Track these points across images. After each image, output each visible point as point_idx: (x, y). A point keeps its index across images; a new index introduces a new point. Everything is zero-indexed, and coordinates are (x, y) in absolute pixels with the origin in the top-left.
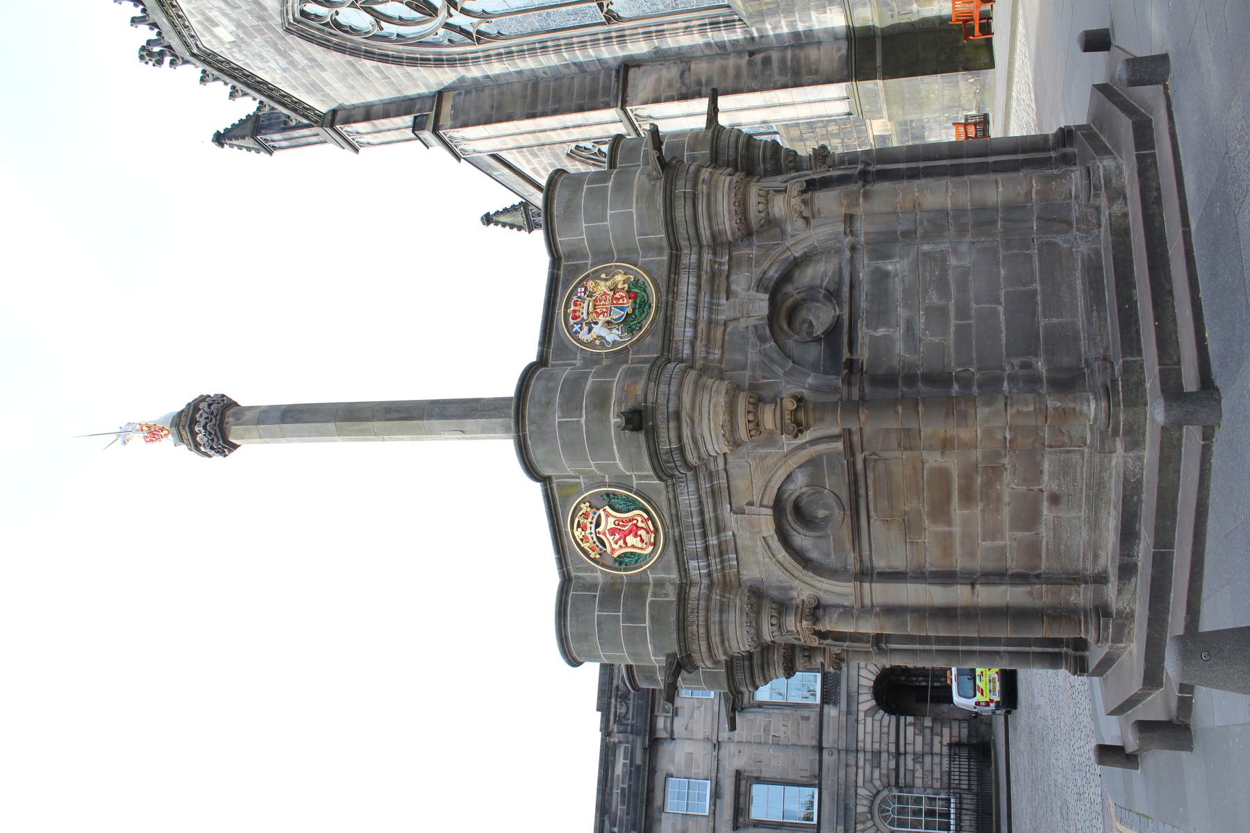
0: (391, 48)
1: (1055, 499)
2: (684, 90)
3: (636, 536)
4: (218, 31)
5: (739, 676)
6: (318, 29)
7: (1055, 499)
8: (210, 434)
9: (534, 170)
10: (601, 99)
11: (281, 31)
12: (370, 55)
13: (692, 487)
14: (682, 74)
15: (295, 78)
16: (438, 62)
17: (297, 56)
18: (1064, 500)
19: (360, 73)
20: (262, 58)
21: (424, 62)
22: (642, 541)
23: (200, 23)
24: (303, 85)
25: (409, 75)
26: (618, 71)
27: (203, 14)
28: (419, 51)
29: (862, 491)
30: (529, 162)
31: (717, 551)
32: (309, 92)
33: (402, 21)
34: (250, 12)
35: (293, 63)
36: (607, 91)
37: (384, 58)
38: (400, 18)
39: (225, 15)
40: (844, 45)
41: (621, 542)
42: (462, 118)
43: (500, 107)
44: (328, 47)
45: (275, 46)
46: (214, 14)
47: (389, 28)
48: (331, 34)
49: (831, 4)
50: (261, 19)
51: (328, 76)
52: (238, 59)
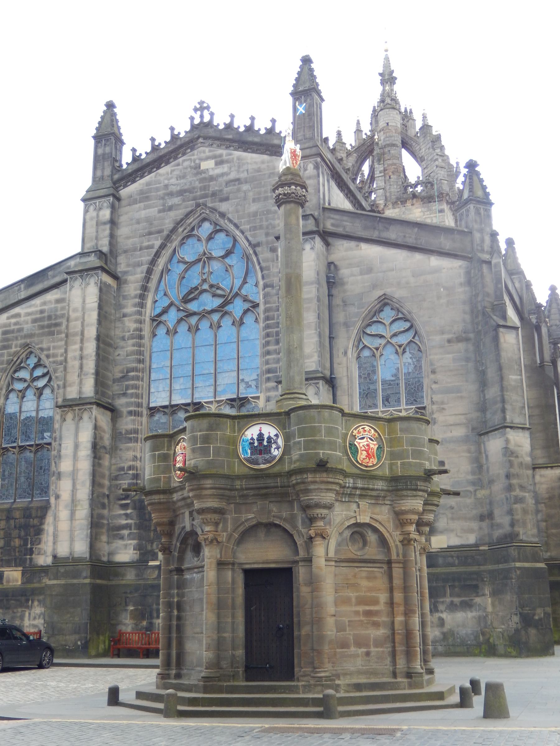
0: (161, 262)
1: (368, 654)
2: (98, 447)
3: (366, 456)
5: (223, 481)
6: (191, 223)
7: (368, 654)
8: (300, 196)
9: (18, 315)
11: (201, 201)
12: (163, 246)
13: (385, 488)
14: (105, 448)
15: (157, 189)
16: (145, 288)
17: (176, 200)
18: (367, 658)
19: (150, 233)
21: (147, 279)
23: (221, 156)
24: (150, 191)
25: (139, 264)
26: (110, 404)
27: (227, 162)
28: (155, 277)
29: (369, 565)
30: (28, 314)
31: (353, 493)
32: (141, 192)
34: (221, 191)
35: (171, 194)
37: (157, 255)
38: (184, 277)
39: (222, 175)
40: (105, 559)
41: (363, 448)
42: (104, 289)
43: (106, 317)
44: (178, 224)
45: (190, 191)
46: (225, 168)
48: (185, 229)
49: (140, 554)
50: (214, 194)
51: (153, 212)
52: (184, 162)
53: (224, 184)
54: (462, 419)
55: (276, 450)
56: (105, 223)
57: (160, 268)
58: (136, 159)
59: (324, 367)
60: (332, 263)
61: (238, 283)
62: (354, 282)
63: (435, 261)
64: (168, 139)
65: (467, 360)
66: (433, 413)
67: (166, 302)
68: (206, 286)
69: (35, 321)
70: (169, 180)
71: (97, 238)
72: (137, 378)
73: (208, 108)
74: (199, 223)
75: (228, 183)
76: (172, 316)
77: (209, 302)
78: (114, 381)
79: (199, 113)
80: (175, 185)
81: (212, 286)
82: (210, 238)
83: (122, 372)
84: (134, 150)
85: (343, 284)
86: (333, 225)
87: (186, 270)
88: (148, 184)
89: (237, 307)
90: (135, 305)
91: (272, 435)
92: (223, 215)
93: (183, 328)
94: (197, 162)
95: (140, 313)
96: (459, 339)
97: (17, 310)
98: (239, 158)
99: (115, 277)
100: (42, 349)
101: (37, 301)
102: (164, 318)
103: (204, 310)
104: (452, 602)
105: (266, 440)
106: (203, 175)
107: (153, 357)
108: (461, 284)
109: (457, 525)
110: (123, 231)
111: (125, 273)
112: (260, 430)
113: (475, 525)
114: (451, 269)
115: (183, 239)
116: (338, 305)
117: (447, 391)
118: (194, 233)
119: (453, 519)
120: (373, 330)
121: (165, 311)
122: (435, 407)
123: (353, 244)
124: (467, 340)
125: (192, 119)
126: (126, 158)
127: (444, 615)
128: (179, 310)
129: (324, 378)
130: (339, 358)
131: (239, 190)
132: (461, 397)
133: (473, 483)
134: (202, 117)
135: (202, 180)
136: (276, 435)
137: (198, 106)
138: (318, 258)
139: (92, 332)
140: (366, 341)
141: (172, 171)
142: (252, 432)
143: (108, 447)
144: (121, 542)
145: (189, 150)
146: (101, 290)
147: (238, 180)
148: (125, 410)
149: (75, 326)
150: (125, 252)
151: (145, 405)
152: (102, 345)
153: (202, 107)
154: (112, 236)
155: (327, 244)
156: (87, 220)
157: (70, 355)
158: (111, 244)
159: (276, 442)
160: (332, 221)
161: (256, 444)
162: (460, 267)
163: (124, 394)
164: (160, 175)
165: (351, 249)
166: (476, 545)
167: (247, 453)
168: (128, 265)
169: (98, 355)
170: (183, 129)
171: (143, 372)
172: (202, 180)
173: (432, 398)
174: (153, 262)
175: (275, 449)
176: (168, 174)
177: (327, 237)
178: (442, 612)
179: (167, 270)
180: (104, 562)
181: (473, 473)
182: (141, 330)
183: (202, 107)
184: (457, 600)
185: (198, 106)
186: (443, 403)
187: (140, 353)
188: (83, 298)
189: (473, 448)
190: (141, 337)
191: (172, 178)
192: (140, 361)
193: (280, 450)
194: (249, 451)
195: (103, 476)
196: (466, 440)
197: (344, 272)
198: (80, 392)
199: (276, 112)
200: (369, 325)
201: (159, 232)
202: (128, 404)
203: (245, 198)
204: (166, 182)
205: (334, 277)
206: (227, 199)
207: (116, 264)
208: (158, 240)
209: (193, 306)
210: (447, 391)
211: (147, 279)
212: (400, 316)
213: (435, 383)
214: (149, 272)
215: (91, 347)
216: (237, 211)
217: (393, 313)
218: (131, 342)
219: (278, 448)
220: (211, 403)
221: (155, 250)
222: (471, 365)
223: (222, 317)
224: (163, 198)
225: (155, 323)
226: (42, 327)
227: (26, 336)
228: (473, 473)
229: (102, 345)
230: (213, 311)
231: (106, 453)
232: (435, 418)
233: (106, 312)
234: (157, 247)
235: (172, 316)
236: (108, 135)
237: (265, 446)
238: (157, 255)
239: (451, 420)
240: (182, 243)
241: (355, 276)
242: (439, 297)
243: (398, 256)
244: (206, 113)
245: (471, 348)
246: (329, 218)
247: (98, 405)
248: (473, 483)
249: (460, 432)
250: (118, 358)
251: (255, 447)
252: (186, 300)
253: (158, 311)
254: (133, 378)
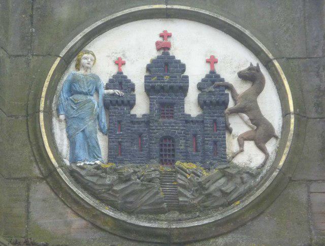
55: (250, 146)
91: (229, 75)
105: (193, 94)
136: (250, 76)
159: (249, 108)
161: (141, 107)
167: (93, 150)
175: (242, 140)
193: (271, 146)
194: (102, 141)
219: (261, 133)
237: (188, 120)
251: (133, 120)
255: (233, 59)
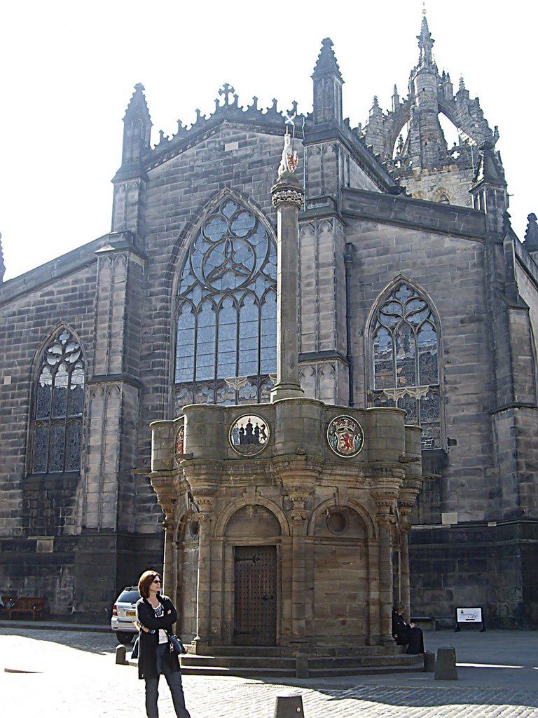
4: (235, 145)
9: (52, 293)
10: (127, 366)
12: (188, 227)
15: (184, 171)
17: (202, 182)
19: (177, 214)
20: (208, 159)
22: (342, 447)
23: (244, 137)
25: (166, 245)
27: (251, 143)
28: (180, 257)
30: (60, 292)
32: (168, 174)
33: (206, 256)
35: (197, 176)
36: (131, 371)
39: (246, 156)
40: (132, 530)
41: (342, 438)
46: (248, 150)
47: (203, 248)
50: (237, 176)
52: (210, 143)
53: (247, 165)
54: (474, 398)
56: (133, 205)
57: (186, 247)
58: (163, 140)
59: (341, 347)
60: (350, 244)
61: (260, 262)
62: (371, 263)
63: (448, 242)
64: (194, 122)
65: (479, 340)
66: (445, 392)
67: (192, 281)
68: (229, 266)
69: (66, 299)
70: (194, 162)
71: (125, 219)
72: (163, 356)
73: (233, 90)
74: (223, 203)
75: (251, 165)
76: (197, 295)
77: (232, 281)
78: (142, 358)
79: (224, 95)
80: (201, 166)
81: (235, 266)
82: (234, 218)
83: (149, 349)
84: (162, 132)
85: (361, 264)
86: (351, 206)
87: (210, 250)
88: (175, 165)
89: (259, 286)
90: (162, 284)
91: (259, 426)
92: (246, 196)
93: (207, 306)
94: (222, 143)
95: (166, 292)
96: (472, 320)
97: (50, 288)
98: (262, 140)
99: (143, 256)
100: (74, 327)
101: (70, 279)
102: (189, 296)
103: (228, 289)
104: (461, 576)
105: (254, 430)
106: (228, 157)
107: (178, 335)
108: (474, 265)
109: (466, 502)
110: (151, 212)
111: (154, 253)
112: (249, 421)
113: (484, 502)
114: (465, 250)
115: (208, 219)
116: (355, 286)
117: (461, 370)
118: (218, 213)
119: (463, 496)
120: (389, 309)
121: (190, 290)
122: (447, 386)
123: (370, 225)
124: (479, 320)
125: (217, 101)
126: (155, 140)
127: (452, 589)
128: (203, 289)
129: (340, 357)
130: (356, 338)
131: (261, 171)
132: (473, 377)
133: (484, 462)
134: (227, 99)
135: (225, 162)
136: (263, 426)
137: (223, 89)
138: (335, 239)
139: (120, 311)
140: (384, 319)
141: (198, 153)
142: (243, 422)
143: (135, 423)
144: (146, 515)
145: (214, 132)
146: (128, 270)
147: (261, 161)
148: (150, 387)
149: (104, 305)
150: (153, 232)
151: (170, 382)
152: (129, 324)
153: (227, 90)
154: (140, 216)
155: (346, 225)
156: (117, 201)
157: (99, 333)
158: (138, 224)
159: (263, 432)
160: (350, 202)
161: (245, 434)
162: (474, 247)
163: (151, 371)
164: (187, 157)
165: (369, 230)
166: (485, 522)
167: (237, 442)
168: (155, 245)
169: (125, 333)
170: (208, 110)
171: (169, 350)
172: (225, 162)
173: (445, 378)
174: (179, 242)
176: (193, 155)
177: (346, 218)
178: (450, 586)
179: (192, 250)
180: (130, 533)
181: (483, 451)
182: (167, 309)
183: (227, 90)
184: (465, 574)
185: (223, 89)
186: (455, 382)
187: (167, 331)
188: (112, 280)
189: (483, 427)
190: (167, 316)
191: (198, 159)
192: (167, 339)
195: (130, 451)
196: (477, 418)
197: (362, 252)
198: (109, 370)
199: (296, 95)
200: (386, 305)
201: (187, 212)
202: (154, 381)
203: (267, 180)
204: (192, 163)
205: (351, 259)
206: (250, 180)
207: (145, 244)
208: (184, 221)
209: (217, 285)
210: (461, 370)
211: (174, 259)
212: (416, 295)
213: (448, 362)
214: (176, 252)
215: (119, 326)
216: (260, 193)
217: (409, 293)
218: (158, 320)
220: (233, 380)
221: (180, 230)
222: (483, 345)
223: (245, 295)
224: (189, 180)
225: (181, 302)
226: (73, 305)
227: (58, 314)
228: (483, 451)
229: (129, 324)
230: (237, 290)
231: (133, 428)
232: (447, 398)
233: (133, 291)
234: (182, 227)
235: (197, 295)
236: (137, 115)
238: (183, 235)
239: (463, 399)
240: (207, 223)
241: (372, 257)
242: (453, 278)
243: (415, 236)
244: (231, 96)
245: (483, 328)
246: (348, 199)
247: (127, 380)
248: (484, 462)
249: (471, 411)
250: (145, 335)
252: (210, 279)
253: (183, 290)
254: (159, 356)
255: (261, 422)
